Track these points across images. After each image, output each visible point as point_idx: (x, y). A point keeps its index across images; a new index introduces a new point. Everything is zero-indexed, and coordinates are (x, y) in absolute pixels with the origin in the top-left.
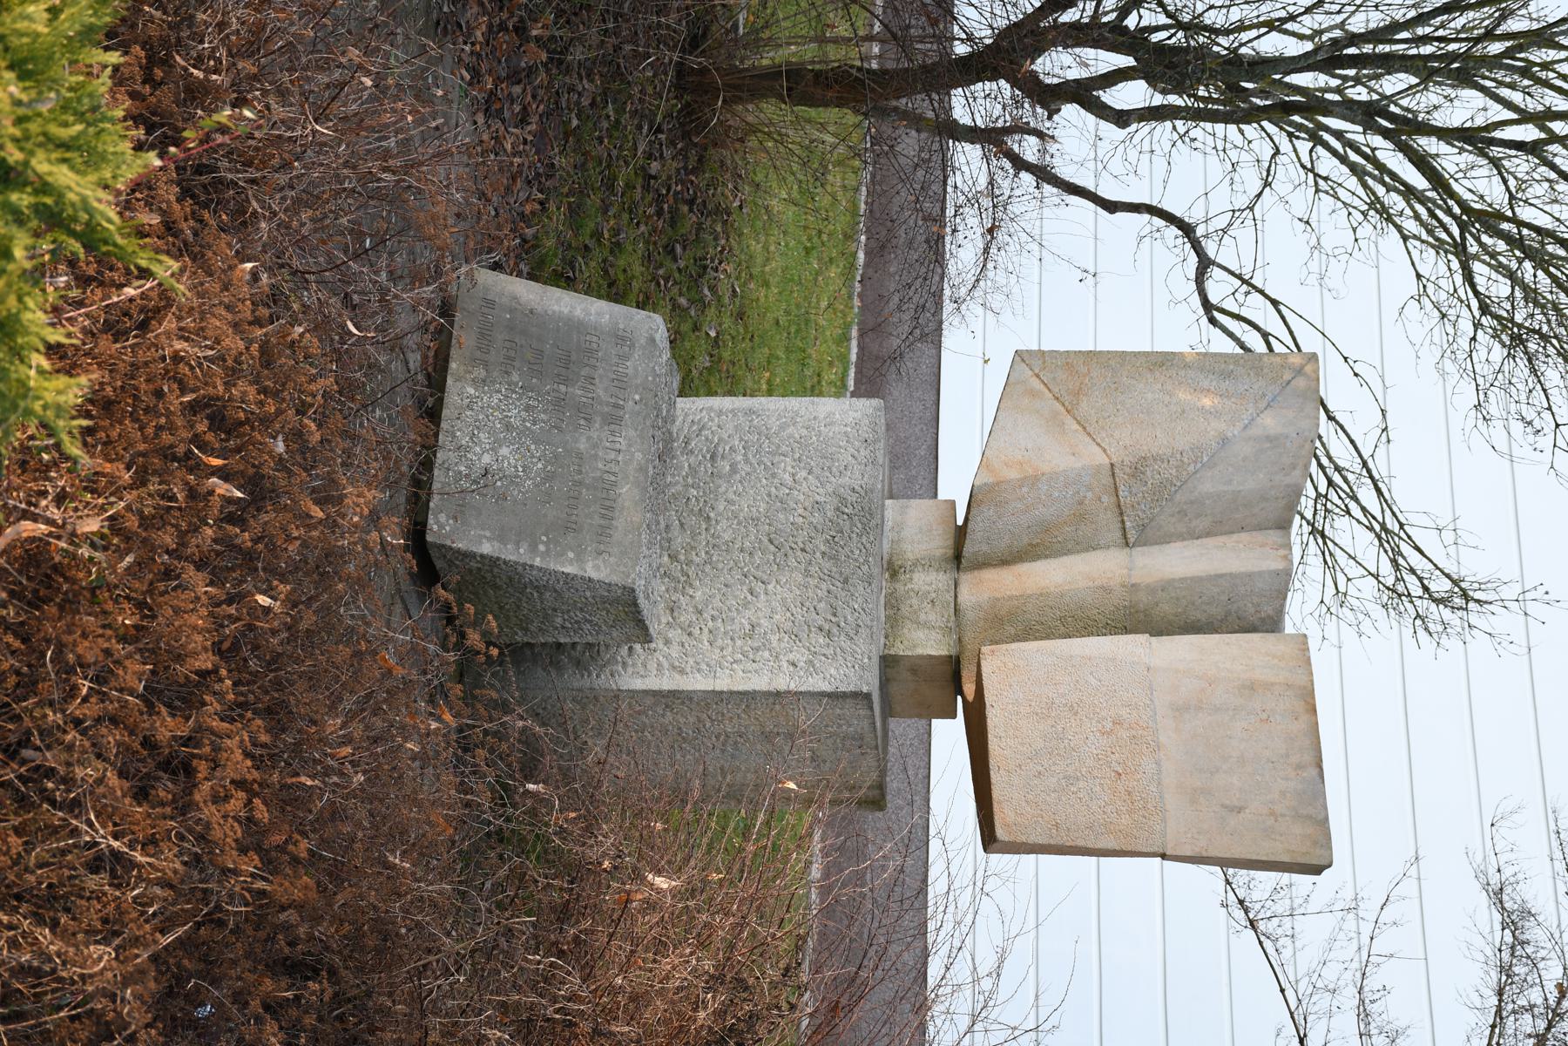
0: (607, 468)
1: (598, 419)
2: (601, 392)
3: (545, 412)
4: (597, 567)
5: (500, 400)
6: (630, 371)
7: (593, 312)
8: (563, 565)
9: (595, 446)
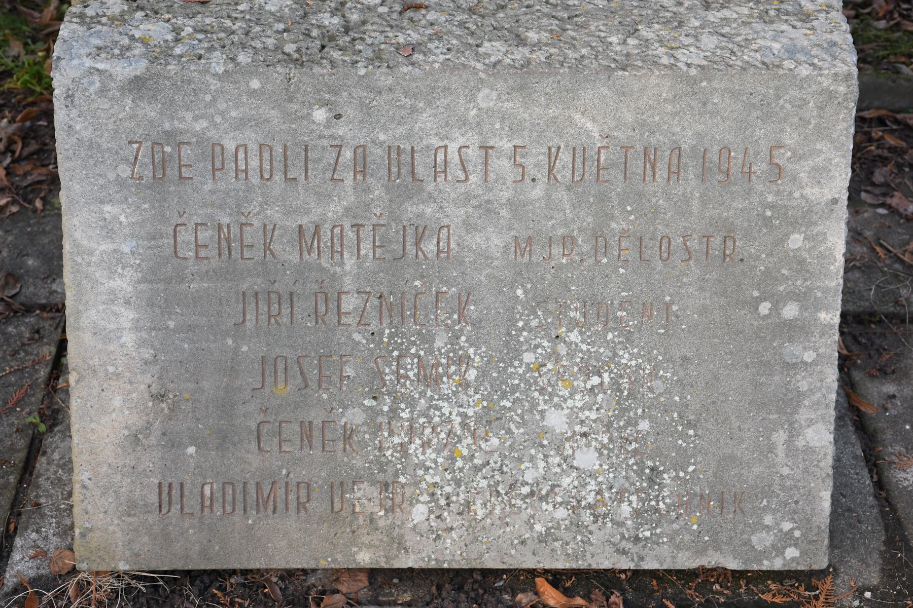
0: (542, 176)
1: (411, 209)
2: (334, 210)
3: (427, 339)
4: (819, 174)
5: (426, 444)
6: (252, 138)
7: (107, 246)
8: (825, 257)
9: (488, 210)
